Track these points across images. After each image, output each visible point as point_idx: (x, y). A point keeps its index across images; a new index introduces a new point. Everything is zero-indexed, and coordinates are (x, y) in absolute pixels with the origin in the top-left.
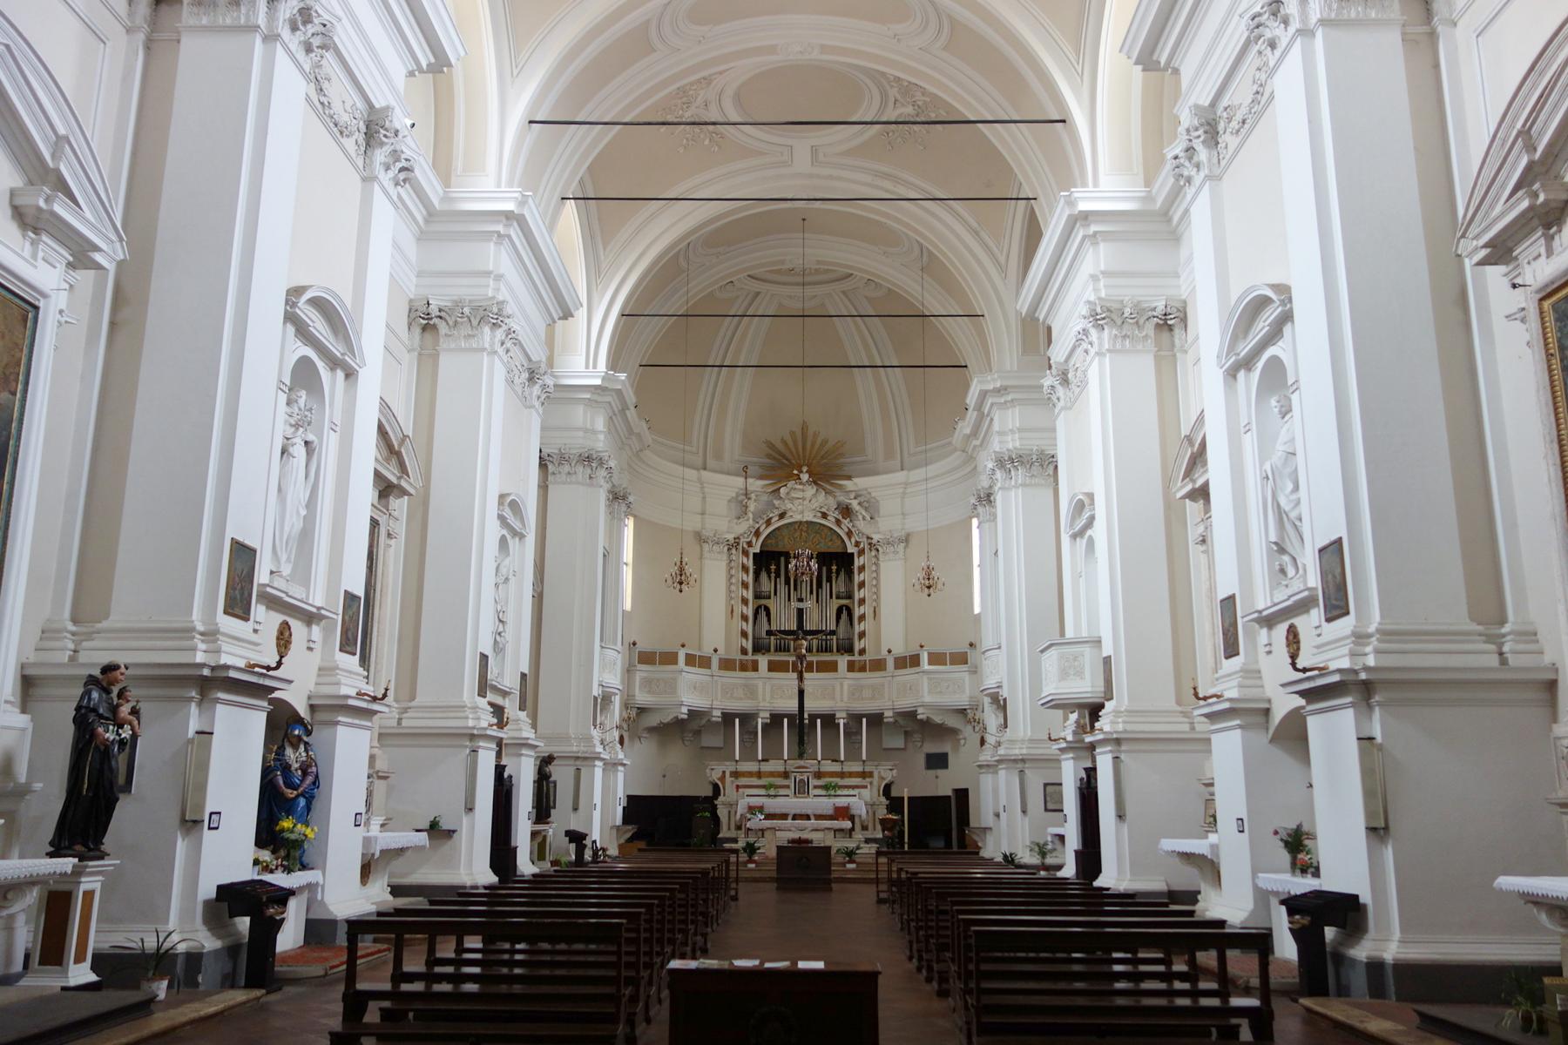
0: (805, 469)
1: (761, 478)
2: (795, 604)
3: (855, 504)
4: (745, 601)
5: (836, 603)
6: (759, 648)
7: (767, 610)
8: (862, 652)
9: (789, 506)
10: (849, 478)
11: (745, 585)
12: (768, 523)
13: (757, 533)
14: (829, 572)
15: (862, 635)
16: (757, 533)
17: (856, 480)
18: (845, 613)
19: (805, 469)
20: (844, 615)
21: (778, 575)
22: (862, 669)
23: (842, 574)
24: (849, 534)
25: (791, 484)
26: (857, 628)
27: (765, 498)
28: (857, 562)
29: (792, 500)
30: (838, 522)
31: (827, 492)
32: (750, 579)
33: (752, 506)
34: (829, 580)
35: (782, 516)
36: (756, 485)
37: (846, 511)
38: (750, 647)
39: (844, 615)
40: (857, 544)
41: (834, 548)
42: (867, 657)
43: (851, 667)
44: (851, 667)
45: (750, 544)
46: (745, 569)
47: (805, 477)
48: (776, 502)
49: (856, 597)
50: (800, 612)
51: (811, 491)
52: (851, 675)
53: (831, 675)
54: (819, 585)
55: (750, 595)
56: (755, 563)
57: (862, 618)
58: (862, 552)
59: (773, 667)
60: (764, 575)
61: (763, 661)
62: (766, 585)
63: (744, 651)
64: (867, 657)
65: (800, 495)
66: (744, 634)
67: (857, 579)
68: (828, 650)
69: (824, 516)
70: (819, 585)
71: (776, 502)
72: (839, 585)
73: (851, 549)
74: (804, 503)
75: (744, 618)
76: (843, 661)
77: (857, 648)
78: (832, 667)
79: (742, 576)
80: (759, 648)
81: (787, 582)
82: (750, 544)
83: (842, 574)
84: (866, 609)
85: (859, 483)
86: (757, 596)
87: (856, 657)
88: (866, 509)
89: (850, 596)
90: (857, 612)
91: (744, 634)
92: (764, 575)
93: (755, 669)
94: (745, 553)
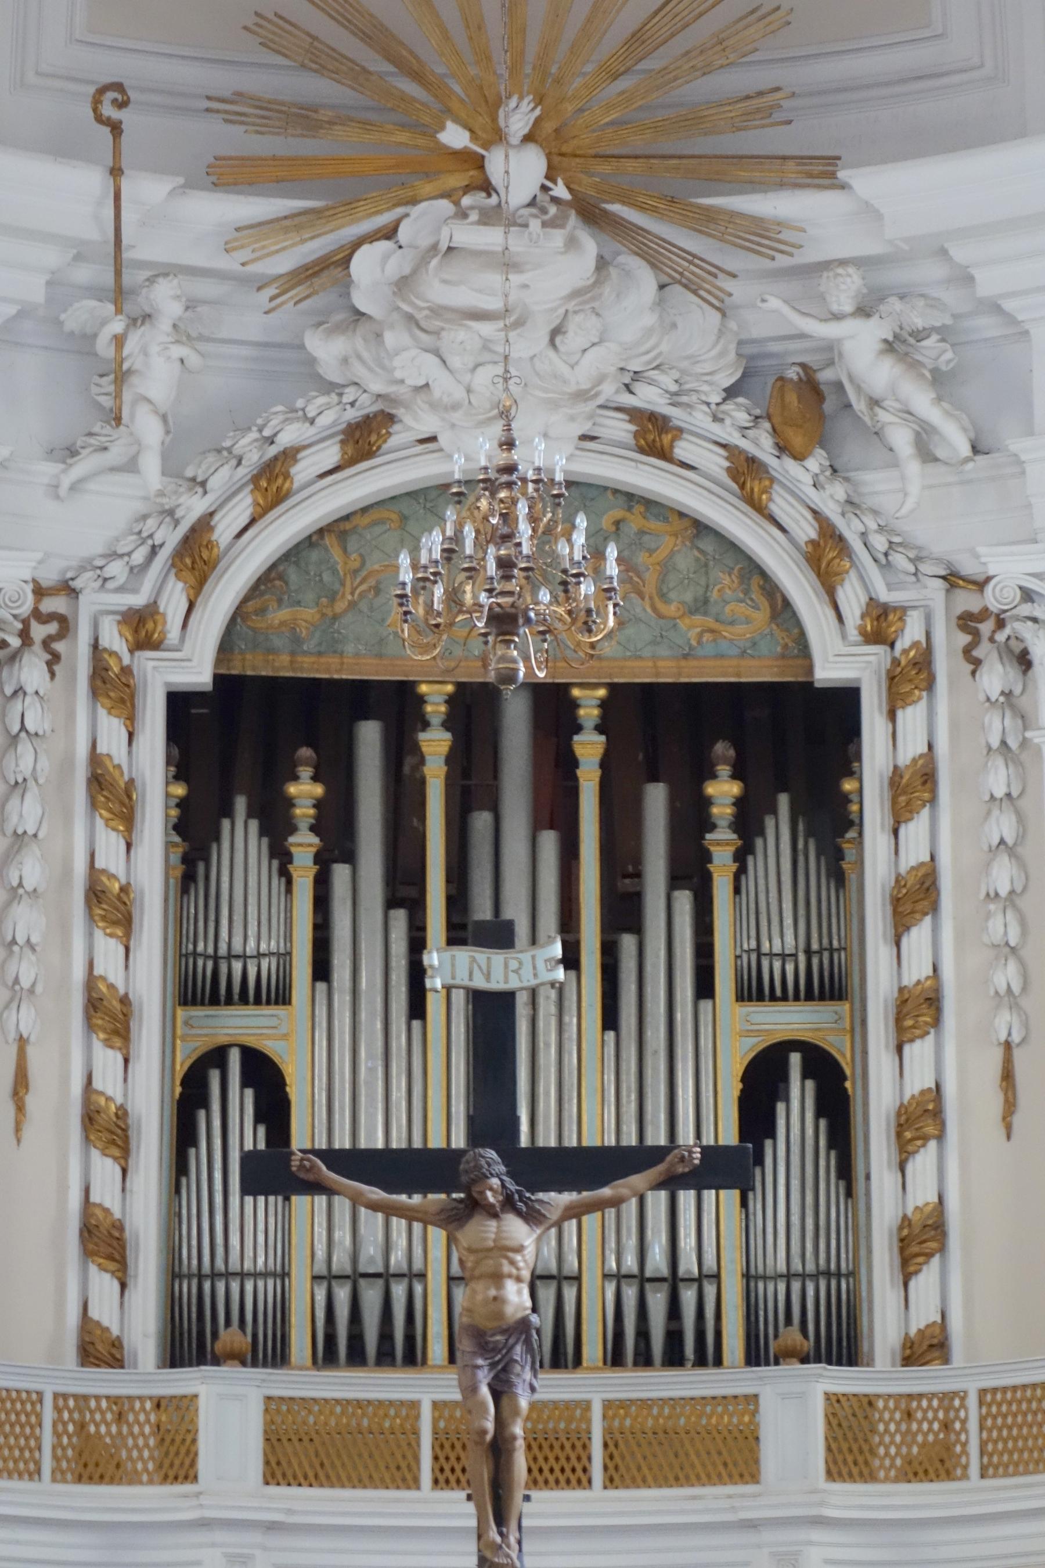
0: (518, 119)
1: (228, 175)
2: (448, 966)
3: (861, 354)
4: (108, 1015)
5: (738, 1032)
6: (189, 1342)
7: (264, 1076)
8: (927, 1348)
9: (410, 364)
10: (821, 171)
11: (109, 905)
12: (272, 483)
13: (196, 557)
14: (691, 821)
15: (922, 1239)
16: (196, 557)
17: (866, 182)
18: (801, 1086)
19: (518, 119)
20: (797, 1107)
21: (337, 842)
22: (937, 1464)
23: (779, 828)
24: (826, 557)
25: (426, 220)
26: (888, 1198)
27: (249, 320)
28: (882, 747)
29: (427, 325)
30: (746, 475)
31: (680, 276)
32: (147, 864)
33: (159, 370)
34: (690, 871)
35: (363, 439)
36: (187, 223)
37: (805, 405)
38: (139, 1319)
39: (797, 1107)
40: (880, 624)
41: (730, 653)
42: (963, 1375)
43: (852, 1446)
44: (852, 1446)
45: (143, 628)
46: (109, 793)
47: (519, 172)
48: (327, 350)
49: (880, 980)
50: (492, 1016)
51: (559, 263)
52: (850, 1499)
53: (713, 1500)
54: (623, 912)
55: (145, 976)
56: (183, 759)
57: (921, 1121)
58: (911, 677)
59: (297, 1453)
60: (241, 841)
61: (229, 1406)
62: (260, 912)
63: (99, 1349)
64: (963, 1375)
65: (479, 290)
66: (103, 1241)
67: (880, 857)
68: (686, 1346)
69: (654, 436)
70: (623, 912)
71: (327, 350)
72: (759, 908)
73: (837, 659)
74: (516, 362)
75: (106, 1128)
76: (794, 1405)
77: (886, 1324)
78: (730, 1452)
79: (87, 841)
80: (189, 1342)
81: (404, 890)
82: (143, 628)
83: (779, 828)
84: (953, 1062)
85: (898, 198)
86: (199, 986)
87: (880, 1377)
88: (940, 381)
89: (830, 983)
90: (882, 1091)
91: (103, 1241)
92: (241, 841)
93: (178, 1462)
94: (112, 686)
